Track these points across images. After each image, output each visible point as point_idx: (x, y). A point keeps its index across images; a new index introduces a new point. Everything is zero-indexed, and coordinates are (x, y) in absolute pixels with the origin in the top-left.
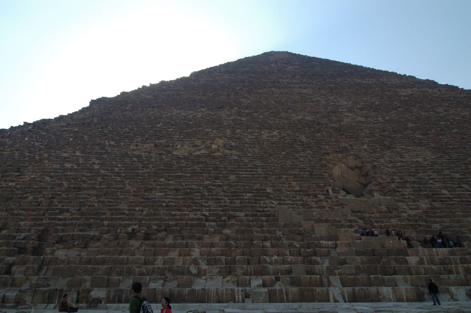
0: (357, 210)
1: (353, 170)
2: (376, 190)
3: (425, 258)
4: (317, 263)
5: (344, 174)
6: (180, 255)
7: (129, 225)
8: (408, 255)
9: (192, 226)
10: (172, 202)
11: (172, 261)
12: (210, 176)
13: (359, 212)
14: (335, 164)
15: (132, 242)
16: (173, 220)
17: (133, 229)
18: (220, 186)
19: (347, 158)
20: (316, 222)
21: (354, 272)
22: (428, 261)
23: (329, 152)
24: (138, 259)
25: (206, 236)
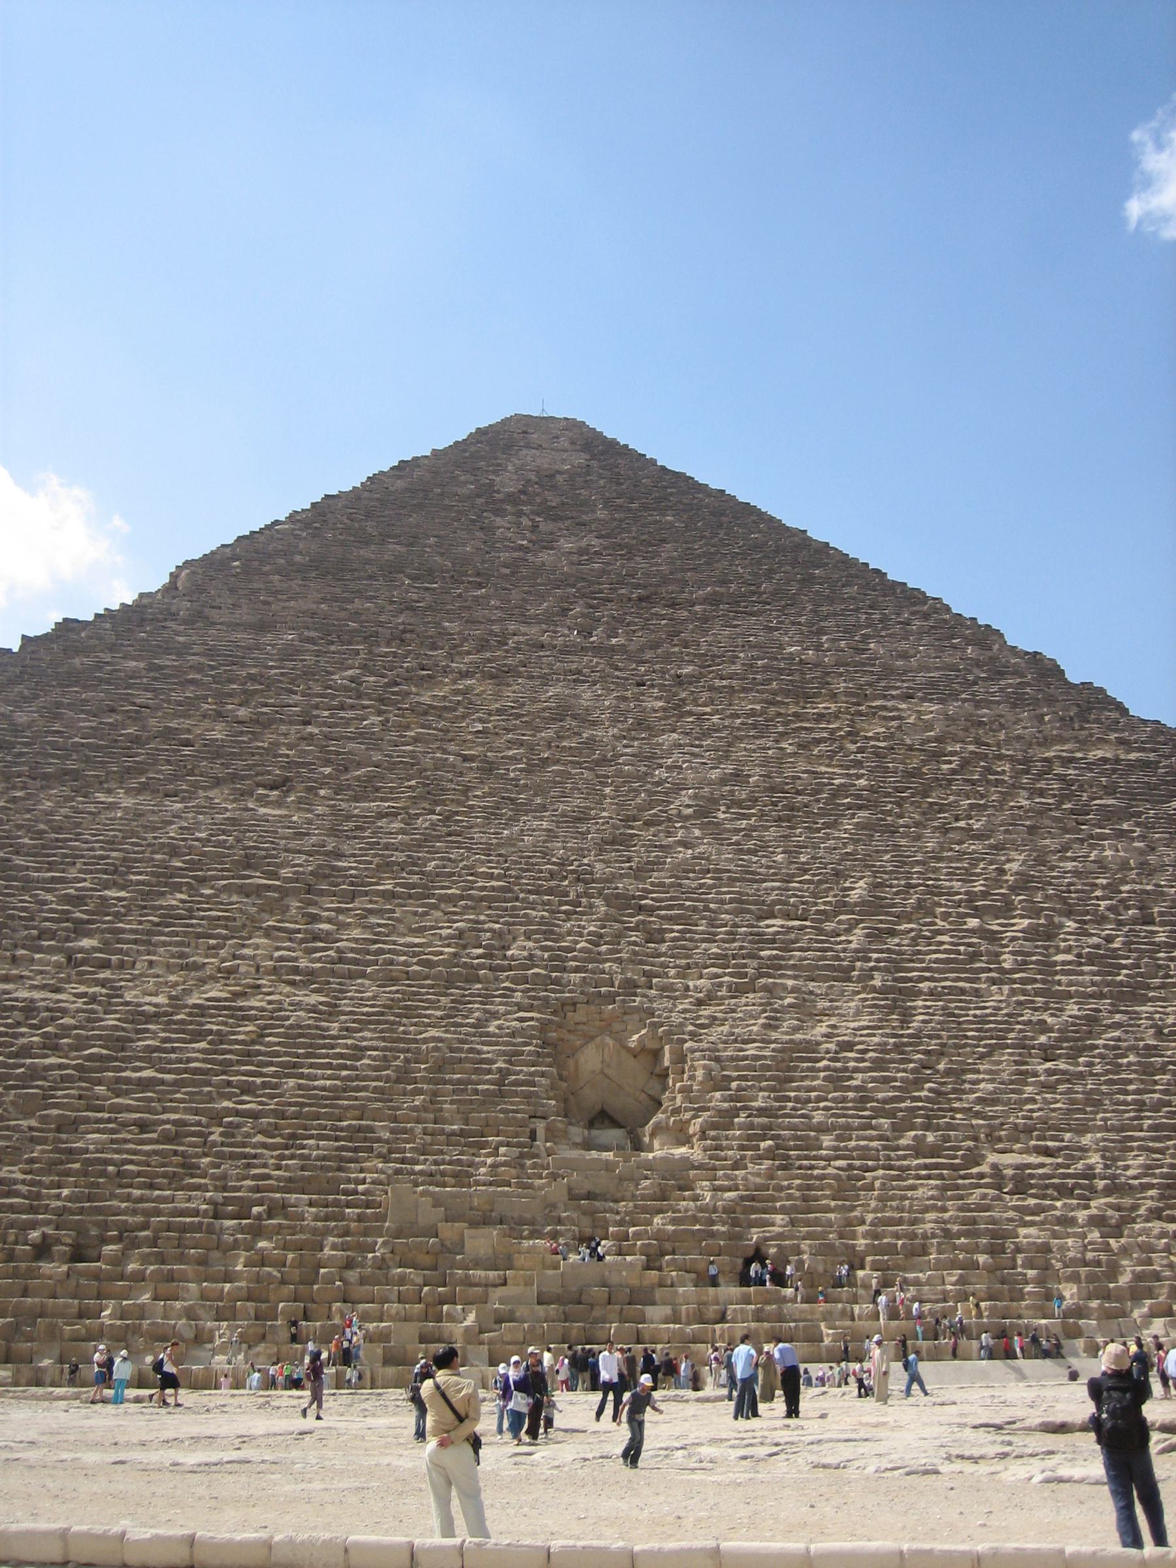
0: (584, 1191)
2: (667, 1128)
4: (451, 1318)
5: (609, 1066)
6: (156, 1298)
7: (34, 1225)
8: (653, 1304)
9: (184, 1229)
10: (131, 1162)
11: (141, 1312)
12: (229, 1084)
13: (590, 1196)
15: (46, 1267)
16: (135, 1212)
17: (44, 1236)
18: (255, 1115)
19: (626, 1018)
20: (473, 1224)
21: (521, 1339)
22: (688, 1315)
24: (66, 1306)
25: (215, 1255)
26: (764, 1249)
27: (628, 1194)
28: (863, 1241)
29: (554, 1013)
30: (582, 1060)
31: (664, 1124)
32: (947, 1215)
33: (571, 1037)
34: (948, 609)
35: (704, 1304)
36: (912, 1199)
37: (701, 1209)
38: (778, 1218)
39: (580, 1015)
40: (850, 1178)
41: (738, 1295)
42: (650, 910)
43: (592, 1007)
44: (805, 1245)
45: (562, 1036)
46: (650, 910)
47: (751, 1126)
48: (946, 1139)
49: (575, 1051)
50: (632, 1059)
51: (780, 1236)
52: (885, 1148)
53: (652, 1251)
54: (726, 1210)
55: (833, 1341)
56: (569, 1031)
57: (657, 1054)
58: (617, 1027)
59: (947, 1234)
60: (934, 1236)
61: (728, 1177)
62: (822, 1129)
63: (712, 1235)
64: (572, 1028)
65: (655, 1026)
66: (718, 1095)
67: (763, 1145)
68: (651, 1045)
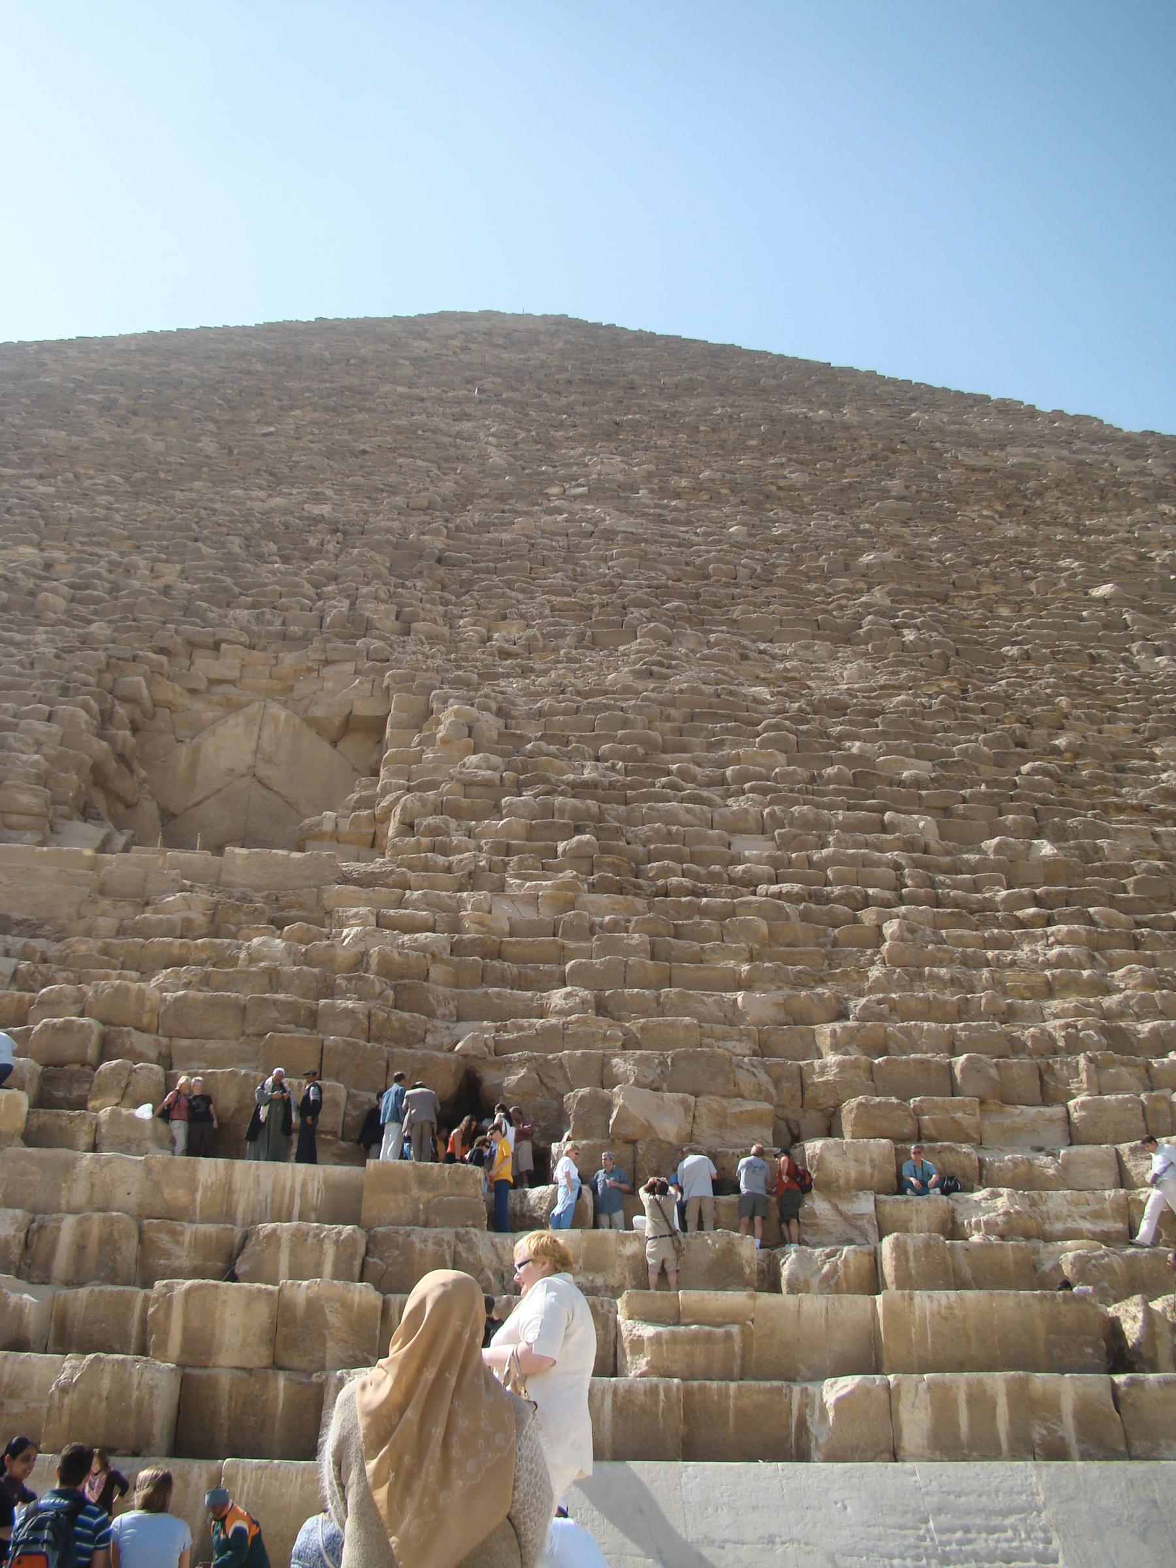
1: (334, 743)
3: (69, 1223)
5: (269, 761)
14: (232, 707)
22: (80, 1248)
23: (223, 633)
26: (489, 1077)
27: (106, 924)
28: (831, 1058)
29: (162, 651)
30: (209, 745)
31: (328, 827)
32: (1111, 1001)
33: (197, 705)
34: (1022, 403)
35: (174, 1215)
36: (998, 963)
37: (307, 959)
38: (557, 997)
39: (227, 665)
40: (805, 916)
41: (314, 1187)
42: (461, 564)
43: (256, 654)
44: (620, 1065)
45: (170, 696)
46: (461, 564)
47: (548, 811)
48: (1089, 855)
49: (198, 728)
50: (327, 748)
51: (556, 1037)
52: (916, 864)
53: (68, 1048)
54: (387, 969)
55: (655, 1369)
56: (193, 692)
57: (375, 728)
58: (304, 687)
59: (1118, 1041)
60: (1074, 1045)
61: (429, 904)
62: (737, 827)
63: (312, 1019)
64: (203, 685)
65: (381, 672)
66: (473, 759)
67: (561, 846)
68: (364, 709)
